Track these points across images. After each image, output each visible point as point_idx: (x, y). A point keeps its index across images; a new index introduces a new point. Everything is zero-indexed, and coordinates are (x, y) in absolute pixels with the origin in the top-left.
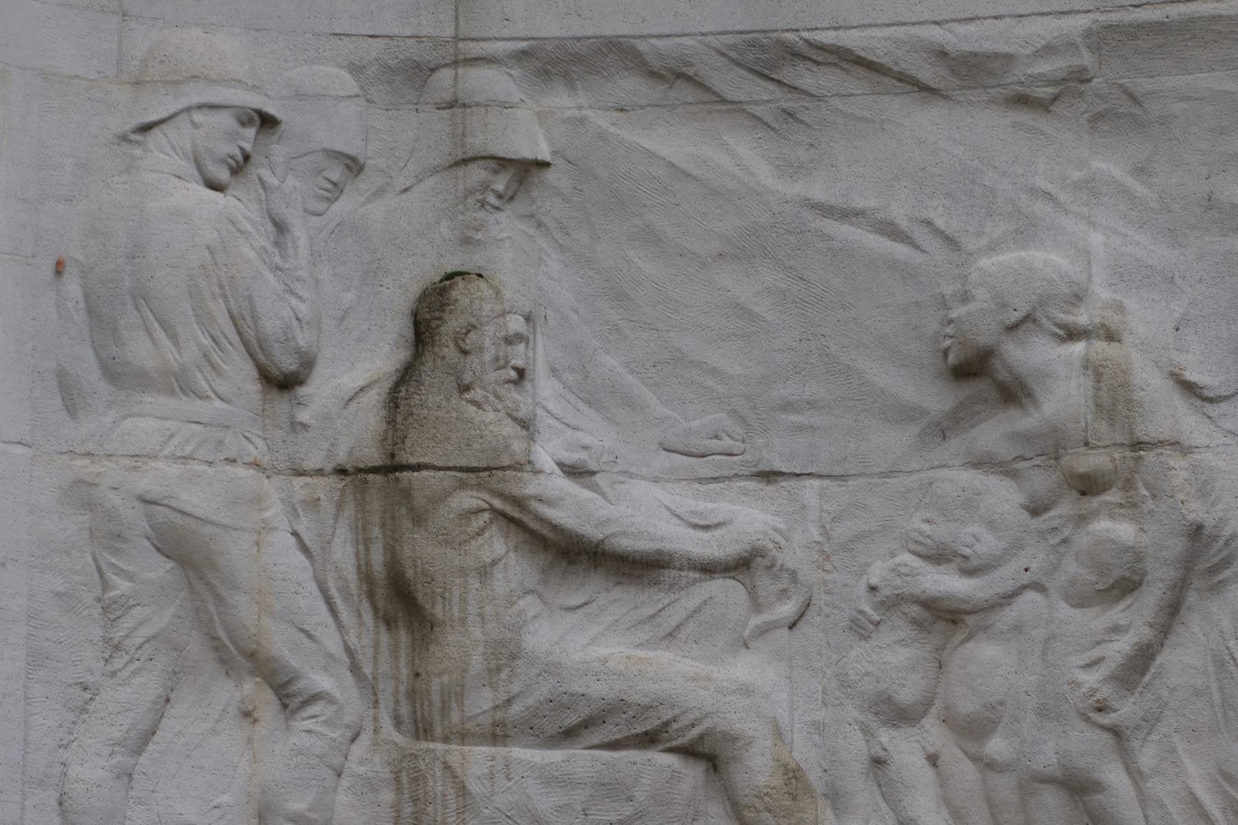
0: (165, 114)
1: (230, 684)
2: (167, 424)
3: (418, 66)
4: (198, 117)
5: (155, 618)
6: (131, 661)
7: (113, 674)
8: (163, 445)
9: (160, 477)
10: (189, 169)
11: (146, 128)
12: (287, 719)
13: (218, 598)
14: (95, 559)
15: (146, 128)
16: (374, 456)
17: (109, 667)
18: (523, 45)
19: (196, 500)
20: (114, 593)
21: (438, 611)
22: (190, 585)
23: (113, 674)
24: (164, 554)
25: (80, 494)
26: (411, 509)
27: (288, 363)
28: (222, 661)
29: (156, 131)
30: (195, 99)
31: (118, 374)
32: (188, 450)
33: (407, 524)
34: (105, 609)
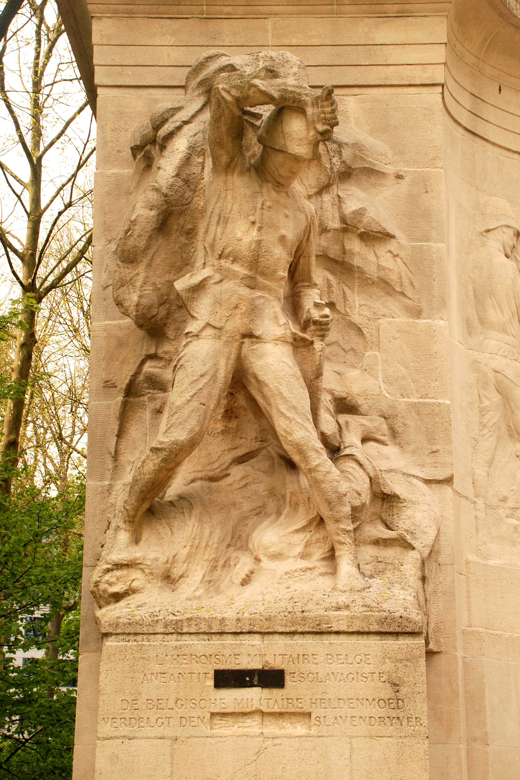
0: (494, 227)
1: (512, 444)
2: (499, 343)
4: (504, 229)
5: (494, 417)
6: (489, 432)
7: (483, 436)
8: (499, 350)
9: (498, 362)
10: (502, 249)
11: (488, 231)
13: (512, 412)
14: (478, 391)
15: (488, 231)
17: (481, 433)
19: (509, 373)
20: (484, 405)
22: (504, 405)
23: (483, 436)
24: (498, 391)
25: (475, 366)
28: (510, 436)
29: (491, 232)
30: (504, 223)
31: (482, 321)
32: (506, 353)
34: (480, 411)
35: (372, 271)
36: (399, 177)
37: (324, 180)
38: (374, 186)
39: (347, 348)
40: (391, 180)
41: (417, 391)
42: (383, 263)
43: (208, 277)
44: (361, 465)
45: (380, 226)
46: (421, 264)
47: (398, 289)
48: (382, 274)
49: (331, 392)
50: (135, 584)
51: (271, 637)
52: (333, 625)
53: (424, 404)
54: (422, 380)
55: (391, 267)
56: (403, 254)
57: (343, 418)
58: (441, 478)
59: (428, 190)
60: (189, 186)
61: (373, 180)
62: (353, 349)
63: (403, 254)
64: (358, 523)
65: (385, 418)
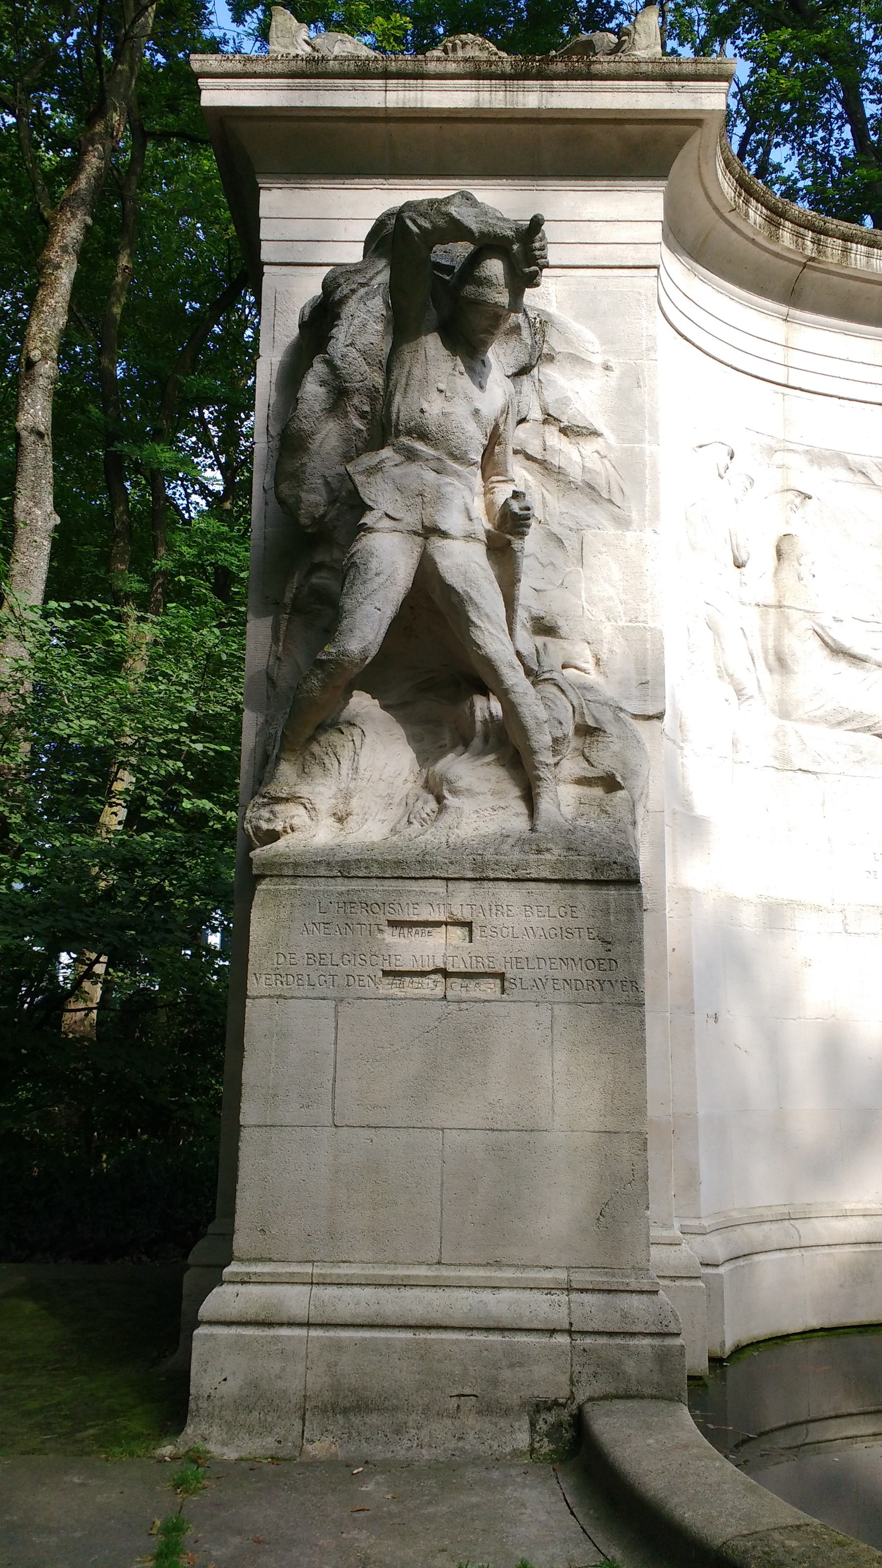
3: (771, 448)
12: (739, 704)
16: (772, 601)
18: (808, 448)
21: (796, 669)
26: (789, 624)
27: (745, 558)
28: (720, 677)
33: (786, 630)
35: (575, 473)
36: (607, 368)
37: (524, 359)
38: (580, 376)
39: (545, 561)
40: (599, 372)
41: (625, 613)
42: (589, 465)
43: (387, 458)
44: (563, 691)
45: (587, 420)
46: (633, 467)
47: (605, 496)
48: (587, 477)
49: (528, 609)
50: (296, 822)
51: (457, 883)
52: (533, 871)
53: (633, 628)
54: (631, 601)
55: (598, 470)
56: (611, 456)
57: (540, 640)
58: (651, 714)
59: (642, 384)
60: (365, 359)
61: (578, 369)
62: (552, 563)
63: (612, 455)
64: (559, 758)
65: (589, 643)
